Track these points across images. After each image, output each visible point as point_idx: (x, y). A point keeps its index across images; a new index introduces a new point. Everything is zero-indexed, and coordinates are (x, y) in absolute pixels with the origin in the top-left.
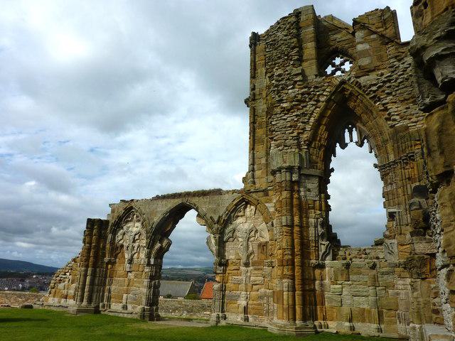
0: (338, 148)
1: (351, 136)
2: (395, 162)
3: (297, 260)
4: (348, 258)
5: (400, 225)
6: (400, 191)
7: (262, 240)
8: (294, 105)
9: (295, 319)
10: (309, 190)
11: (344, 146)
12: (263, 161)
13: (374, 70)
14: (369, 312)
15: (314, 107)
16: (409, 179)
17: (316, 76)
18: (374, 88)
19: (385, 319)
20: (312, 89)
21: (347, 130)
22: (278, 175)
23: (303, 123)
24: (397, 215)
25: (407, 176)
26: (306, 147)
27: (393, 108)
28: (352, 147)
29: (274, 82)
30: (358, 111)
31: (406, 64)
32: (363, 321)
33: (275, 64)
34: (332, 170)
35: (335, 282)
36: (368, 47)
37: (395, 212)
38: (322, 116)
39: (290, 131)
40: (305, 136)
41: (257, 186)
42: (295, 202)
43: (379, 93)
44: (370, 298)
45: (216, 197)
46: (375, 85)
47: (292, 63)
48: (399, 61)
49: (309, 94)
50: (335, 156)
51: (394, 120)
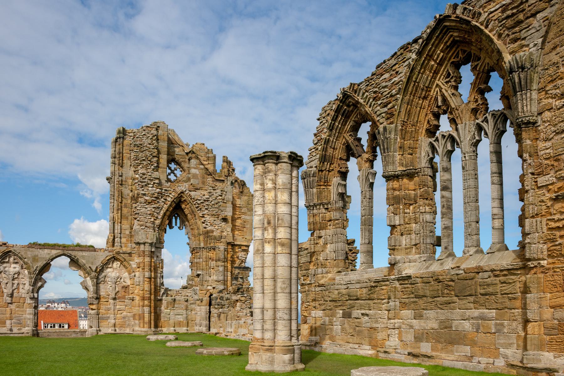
3: (153, 297)
4: (174, 296)
7: (124, 284)
11: (171, 227)
12: (127, 232)
14: (183, 322)
18: (199, 202)
19: (190, 325)
20: (163, 191)
22: (142, 246)
24: (201, 276)
27: (207, 218)
28: (176, 228)
30: (186, 211)
32: (180, 327)
36: (198, 173)
38: (167, 210)
40: (158, 222)
41: (124, 249)
42: (153, 264)
46: (199, 200)
51: (207, 225)
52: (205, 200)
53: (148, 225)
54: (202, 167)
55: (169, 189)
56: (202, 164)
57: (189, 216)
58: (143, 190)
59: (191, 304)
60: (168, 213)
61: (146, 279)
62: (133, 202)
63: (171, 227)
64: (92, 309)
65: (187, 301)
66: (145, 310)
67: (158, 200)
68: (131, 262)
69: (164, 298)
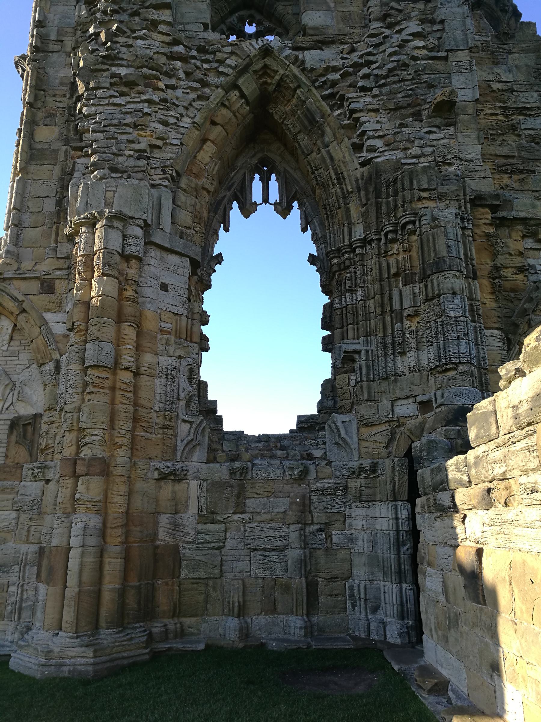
0: (235, 212)
2: (365, 242)
5: (368, 380)
8: (146, 77)
9: (96, 627)
10: (164, 287)
11: (248, 209)
13: (332, 42)
15: (193, 95)
16: (397, 275)
17: (206, 27)
21: (257, 176)
23: (165, 123)
25: (393, 270)
27: (371, 123)
28: (265, 213)
30: (291, 125)
31: (404, 33)
34: (219, 259)
37: (359, 352)
39: (130, 137)
43: (342, 89)
46: (335, 69)
48: (390, 26)
50: (227, 230)
52: (357, 66)
57: (304, 141)
68: (48, 316)
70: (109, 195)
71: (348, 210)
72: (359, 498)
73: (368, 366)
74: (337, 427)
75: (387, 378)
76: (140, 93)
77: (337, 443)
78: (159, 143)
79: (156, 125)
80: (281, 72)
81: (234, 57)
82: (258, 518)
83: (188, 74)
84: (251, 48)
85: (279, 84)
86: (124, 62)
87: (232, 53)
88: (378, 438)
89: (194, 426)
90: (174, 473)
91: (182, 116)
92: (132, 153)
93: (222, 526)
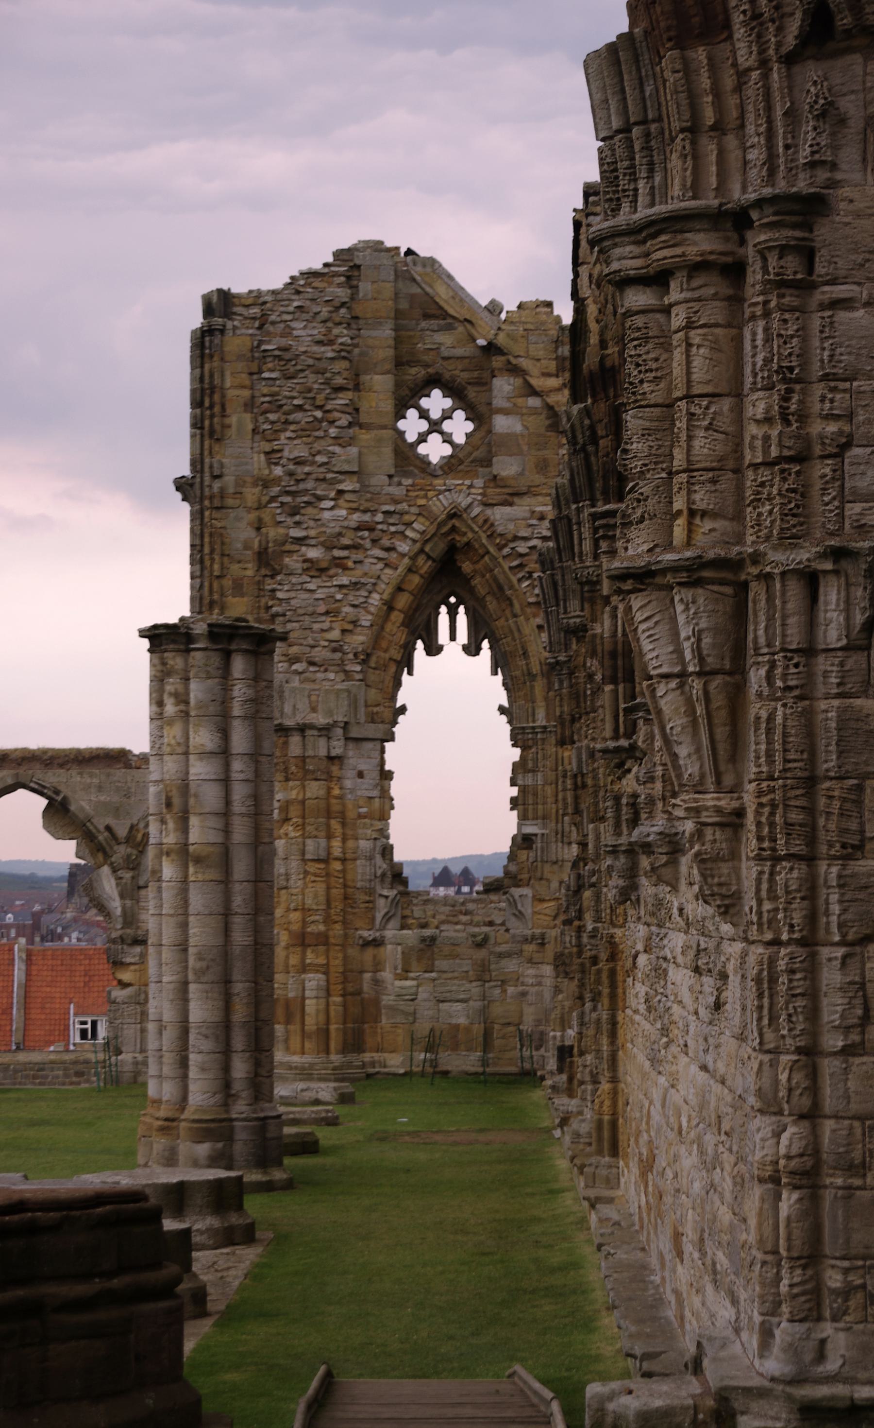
1: (452, 626)
5: (542, 861)
6: (549, 790)
8: (335, 558)
10: (361, 775)
11: (433, 649)
18: (522, 547)
21: (443, 609)
22: (295, 739)
23: (354, 606)
26: (358, 668)
29: (278, 471)
33: (287, 422)
34: (403, 710)
35: (405, 973)
37: (536, 835)
39: (326, 626)
40: (359, 640)
44: (471, 1003)
45: (119, 773)
47: (333, 432)
49: (371, 529)
50: (410, 673)
53: (320, 654)
54: (534, 402)
55: (404, 506)
56: (534, 392)
58: (298, 524)
59: (501, 956)
60: (403, 601)
61: (312, 868)
62: (264, 571)
63: (433, 649)
64: (123, 985)
65: (482, 943)
66: (308, 985)
67: (359, 556)
69: (389, 933)
70: (314, 698)
71: (532, 687)
72: (530, 961)
73: (542, 848)
74: (514, 901)
75: (556, 863)
76: (332, 577)
77: (514, 914)
78: (350, 627)
79: (347, 609)
80: (470, 535)
81: (421, 519)
82: (445, 976)
83: (374, 541)
84: (438, 503)
85: (468, 544)
86: (313, 542)
87: (419, 514)
88: (547, 911)
89: (390, 899)
90: (374, 940)
91: (370, 592)
92: (326, 644)
93: (414, 983)
